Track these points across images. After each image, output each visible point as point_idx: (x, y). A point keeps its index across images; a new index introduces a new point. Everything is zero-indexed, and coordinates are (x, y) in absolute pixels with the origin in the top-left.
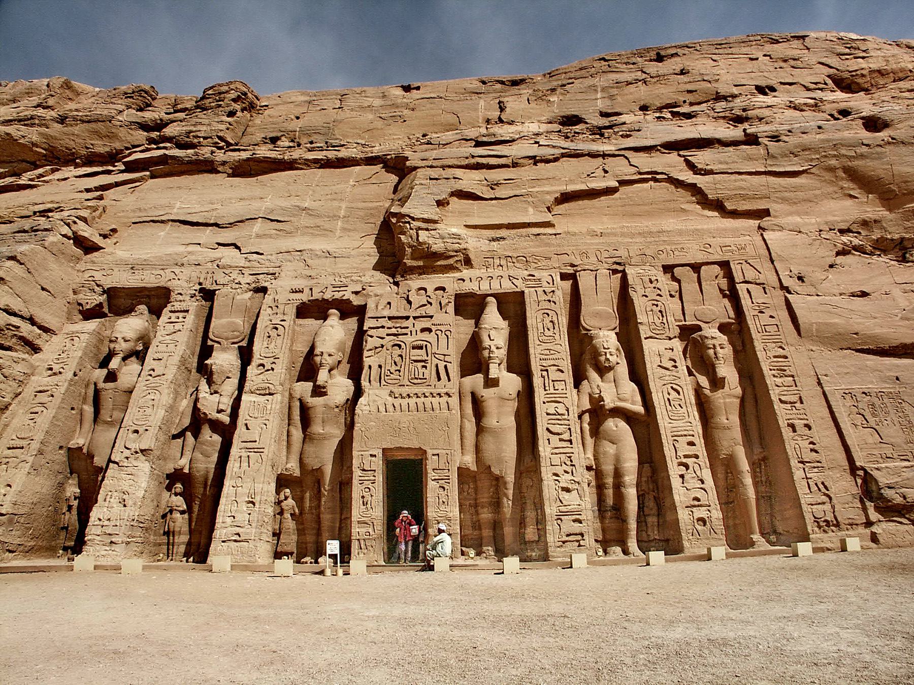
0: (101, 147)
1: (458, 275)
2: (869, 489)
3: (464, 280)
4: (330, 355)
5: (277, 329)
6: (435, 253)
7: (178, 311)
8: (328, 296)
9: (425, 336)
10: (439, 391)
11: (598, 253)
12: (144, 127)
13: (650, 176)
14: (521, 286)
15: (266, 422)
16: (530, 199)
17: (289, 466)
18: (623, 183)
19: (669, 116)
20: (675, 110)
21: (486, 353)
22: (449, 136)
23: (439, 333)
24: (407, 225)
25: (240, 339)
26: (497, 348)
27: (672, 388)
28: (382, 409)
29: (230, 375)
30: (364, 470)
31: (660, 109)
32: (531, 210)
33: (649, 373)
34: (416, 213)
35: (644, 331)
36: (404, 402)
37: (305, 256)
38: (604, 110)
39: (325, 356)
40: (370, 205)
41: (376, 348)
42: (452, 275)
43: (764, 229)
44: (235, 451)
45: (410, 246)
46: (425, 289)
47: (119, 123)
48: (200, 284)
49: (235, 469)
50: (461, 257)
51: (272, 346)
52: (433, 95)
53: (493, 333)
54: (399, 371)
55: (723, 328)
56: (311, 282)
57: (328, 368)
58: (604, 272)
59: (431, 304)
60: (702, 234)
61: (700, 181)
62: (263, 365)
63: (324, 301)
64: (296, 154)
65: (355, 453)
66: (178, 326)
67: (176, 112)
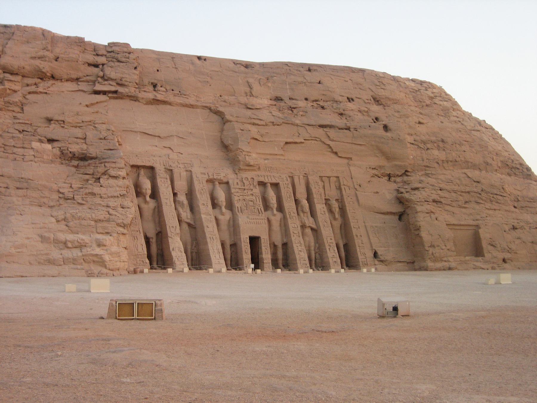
0: (74, 76)
1: (255, 173)
2: (375, 255)
8: (215, 177)
9: (251, 197)
12: (90, 65)
19: (316, 105)
20: (318, 103)
22: (232, 99)
32: (276, 149)
35: (316, 201)
36: (253, 221)
38: (291, 97)
47: (81, 63)
52: (217, 70)
55: (337, 200)
58: (301, 177)
60: (331, 165)
61: (331, 143)
63: (215, 179)
64: (171, 98)
65: (242, 237)
66: (166, 185)
67: (98, 55)
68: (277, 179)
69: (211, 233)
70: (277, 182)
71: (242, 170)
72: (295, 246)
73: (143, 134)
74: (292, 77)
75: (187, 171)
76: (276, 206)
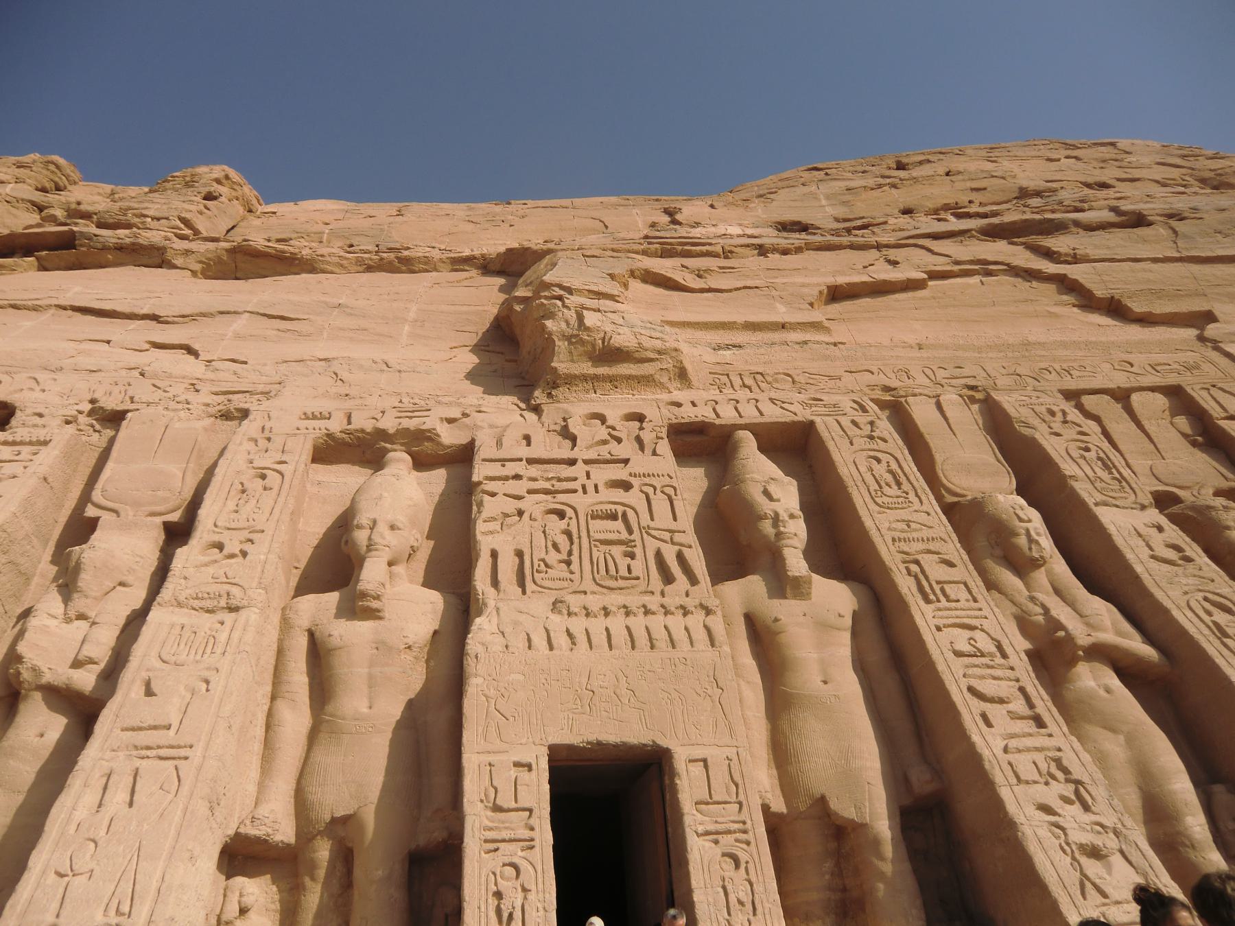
3: (679, 405)
4: (393, 527)
5: (263, 477)
6: (618, 349)
7: (21, 443)
8: (389, 424)
10: (679, 601)
11: (926, 370)
13: (976, 267)
14: (803, 414)
15: (206, 674)
16: (774, 293)
17: (263, 811)
18: (934, 275)
21: (767, 527)
23: (650, 490)
24: (559, 303)
25: (170, 506)
26: (792, 516)
27: (1206, 599)
28: (539, 640)
29: (129, 579)
30: (497, 809)
31: (936, 212)
32: (781, 308)
33: (1139, 569)
34: (575, 283)
36: (597, 626)
37: (335, 366)
38: (841, 216)
39: (382, 528)
40: (465, 308)
41: (506, 515)
42: (650, 396)
43: (1215, 342)
44: (93, 755)
45: (568, 338)
46: (602, 419)
48: (92, 401)
49: (81, 814)
50: (668, 363)
51: (247, 510)
53: (772, 489)
54: (568, 563)
56: (348, 405)
57: (385, 556)
58: (950, 398)
59: (619, 440)
62: (220, 546)
63: (381, 434)
65: (470, 760)
68: (796, 408)
69: (143, 738)
70: (799, 418)
71: (570, 380)
72: (1019, 803)
73: (70, 312)
74: (843, 184)
75: (226, 416)
76: (797, 531)
